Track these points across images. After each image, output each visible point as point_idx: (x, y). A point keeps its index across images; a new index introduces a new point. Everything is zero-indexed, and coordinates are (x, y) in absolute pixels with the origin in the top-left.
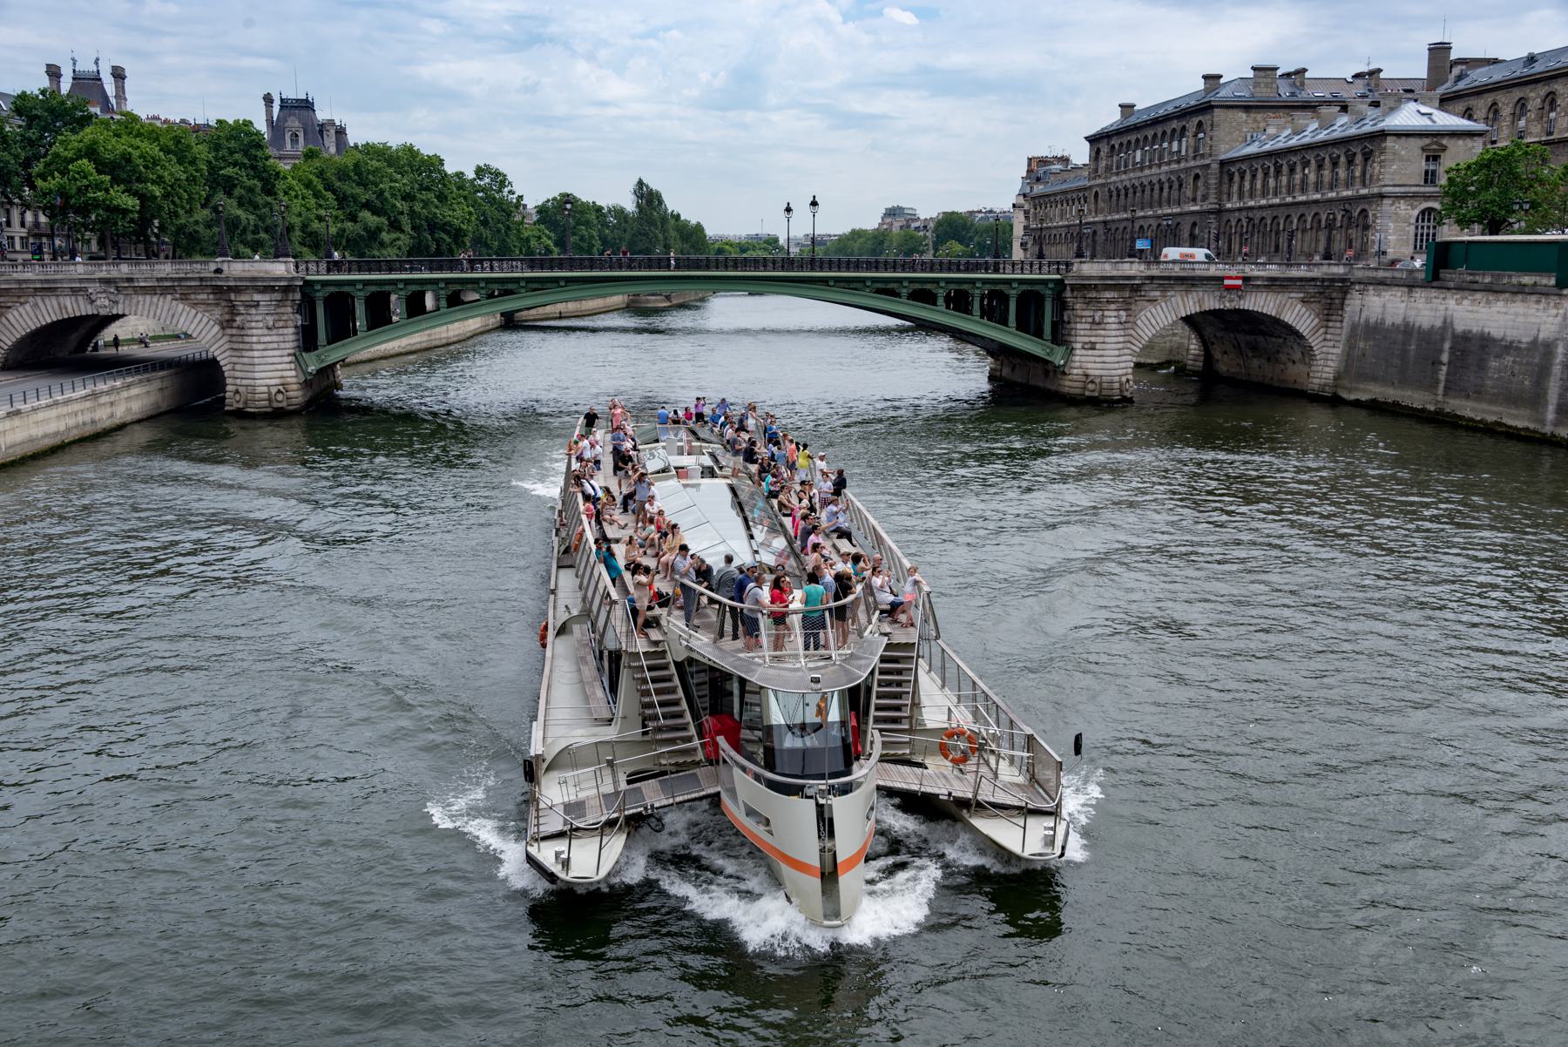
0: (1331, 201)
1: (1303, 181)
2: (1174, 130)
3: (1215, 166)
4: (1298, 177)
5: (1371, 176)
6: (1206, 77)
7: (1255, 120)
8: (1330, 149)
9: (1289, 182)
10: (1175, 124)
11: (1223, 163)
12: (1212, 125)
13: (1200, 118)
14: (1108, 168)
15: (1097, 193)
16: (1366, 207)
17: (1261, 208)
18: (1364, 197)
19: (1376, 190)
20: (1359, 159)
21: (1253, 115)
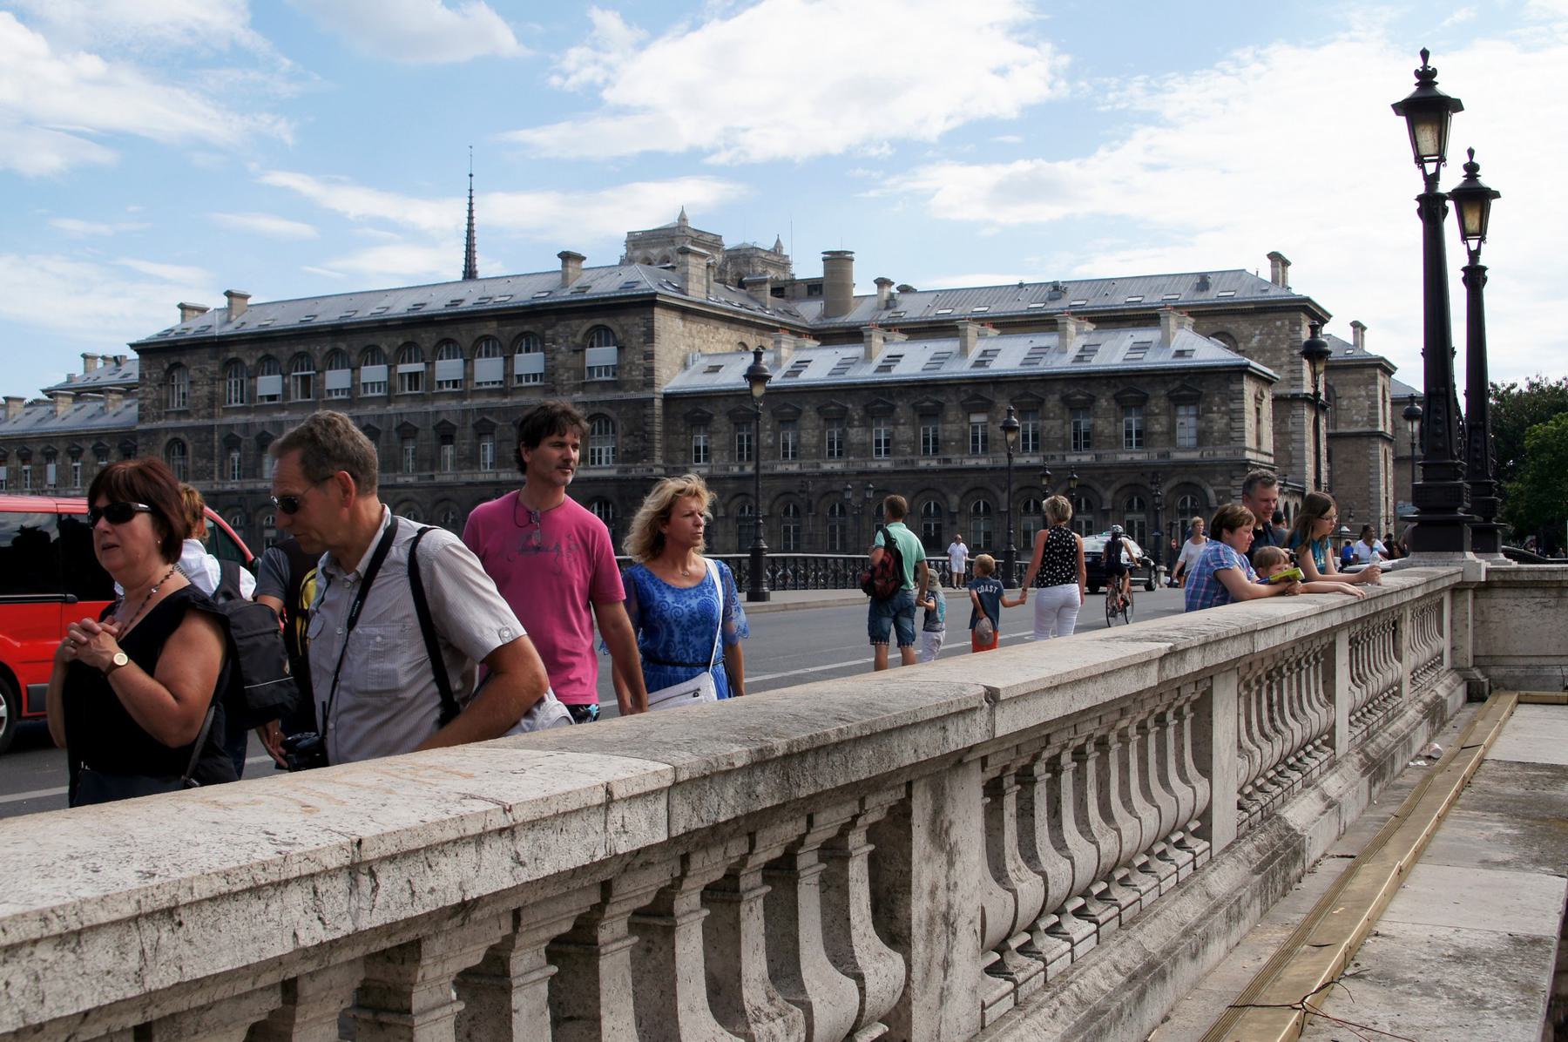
0: (1080, 468)
1: (965, 434)
2: (486, 338)
3: (658, 403)
4: (951, 428)
5: (1202, 438)
6: (566, 257)
7: (691, 335)
8: (1058, 387)
9: (917, 435)
10: (491, 328)
11: (669, 398)
12: (650, 336)
13: (599, 321)
14: (212, 400)
15: (175, 441)
16: (1196, 479)
17: (826, 475)
18: (1188, 465)
19: (1221, 454)
20: (1158, 404)
21: (688, 325)
